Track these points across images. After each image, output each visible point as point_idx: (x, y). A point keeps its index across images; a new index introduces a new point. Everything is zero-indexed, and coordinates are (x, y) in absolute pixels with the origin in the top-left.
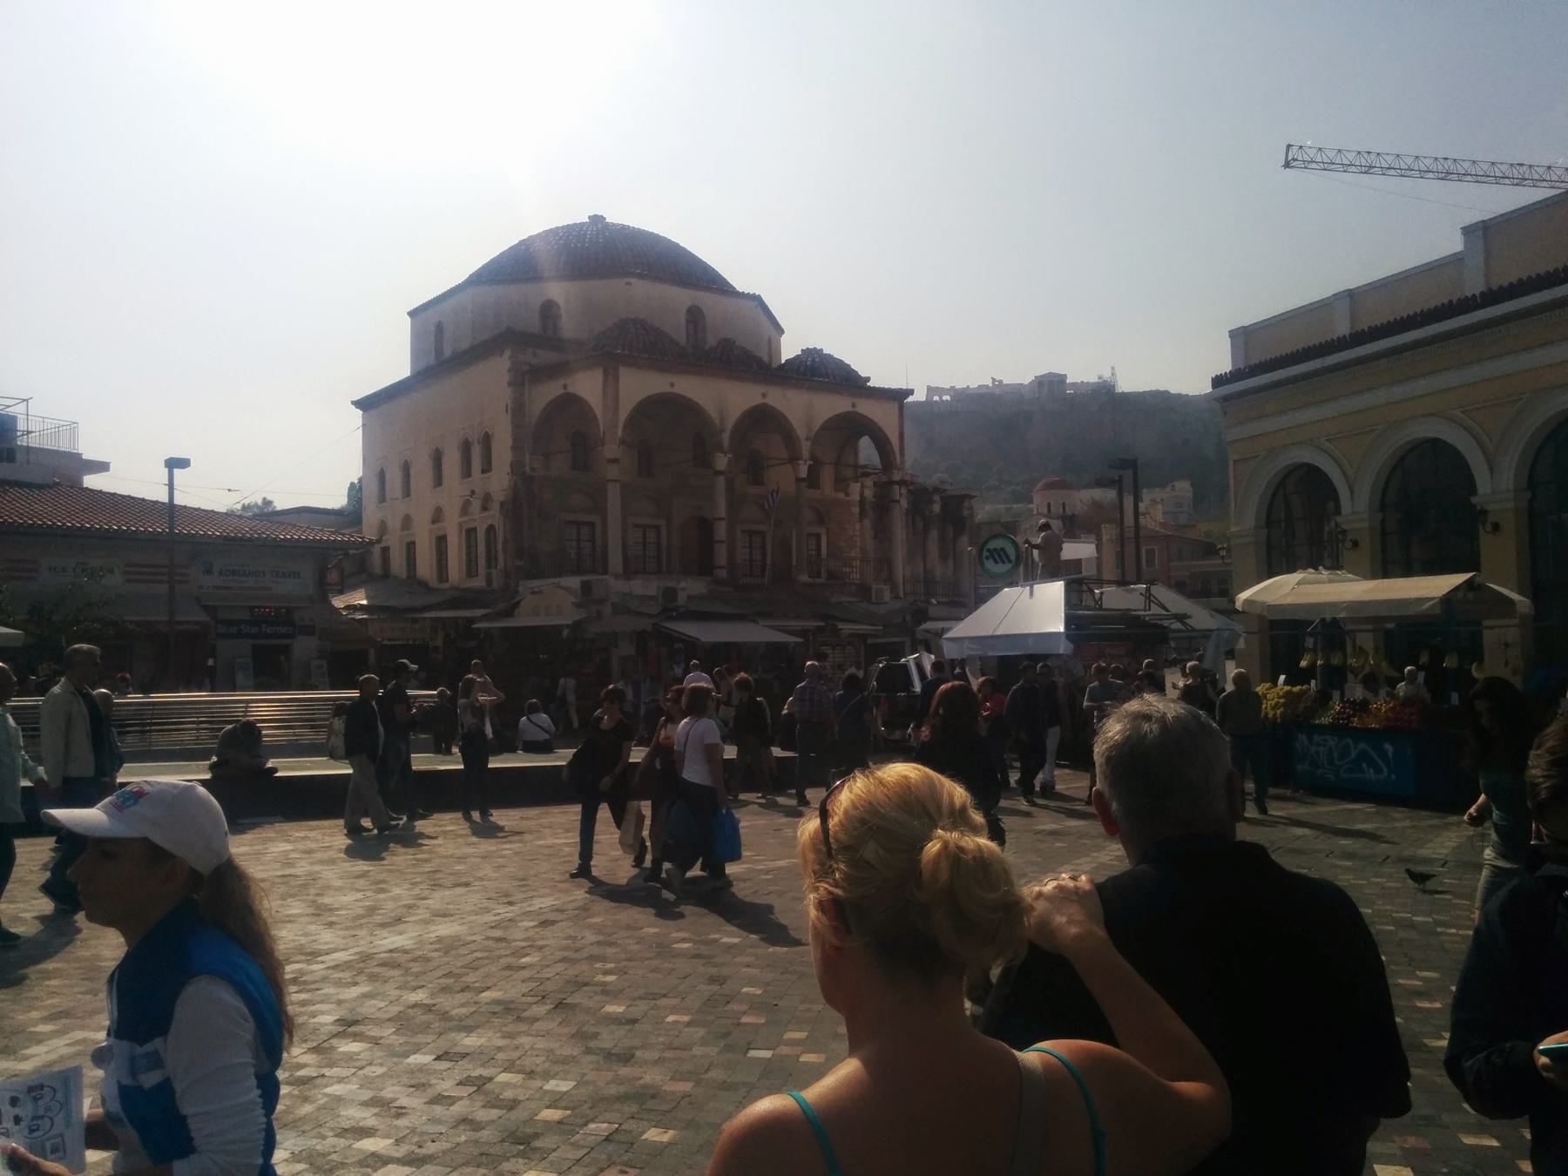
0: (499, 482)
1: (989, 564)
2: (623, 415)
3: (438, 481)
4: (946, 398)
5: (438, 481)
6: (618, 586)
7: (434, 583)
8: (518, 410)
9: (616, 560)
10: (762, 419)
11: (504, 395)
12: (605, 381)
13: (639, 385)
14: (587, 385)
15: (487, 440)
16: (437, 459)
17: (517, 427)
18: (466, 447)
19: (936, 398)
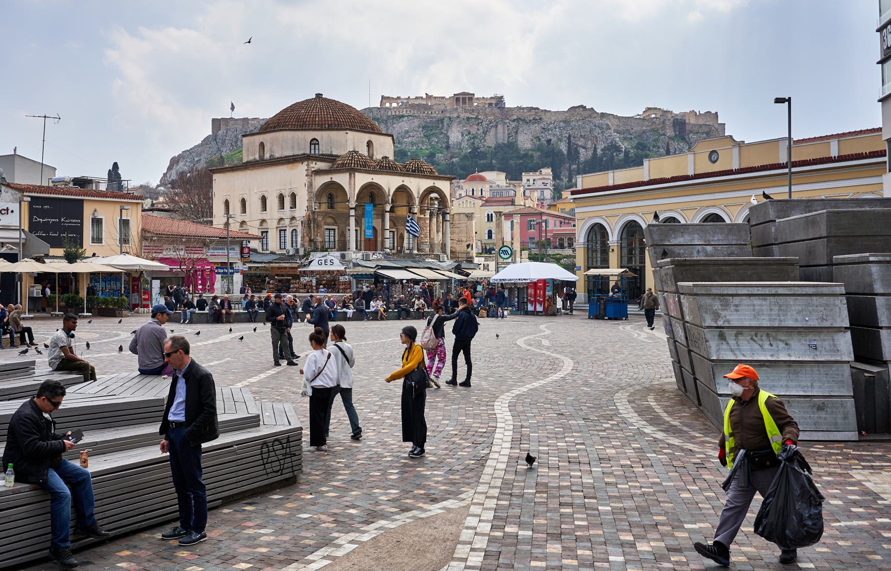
0: (301, 212)
1: (502, 255)
2: (357, 192)
3: (264, 207)
4: (394, 105)
5: (264, 207)
6: (354, 256)
7: (260, 250)
8: (311, 185)
9: (353, 245)
10: (403, 190)
11: (305, 180)
12: (350, 178)
13: (362, 179)
14: (342, 179)
15: (293, 196)
16: (264, 200)
17: (310, 192)
18: (281, 198)
19: (388, 105)
